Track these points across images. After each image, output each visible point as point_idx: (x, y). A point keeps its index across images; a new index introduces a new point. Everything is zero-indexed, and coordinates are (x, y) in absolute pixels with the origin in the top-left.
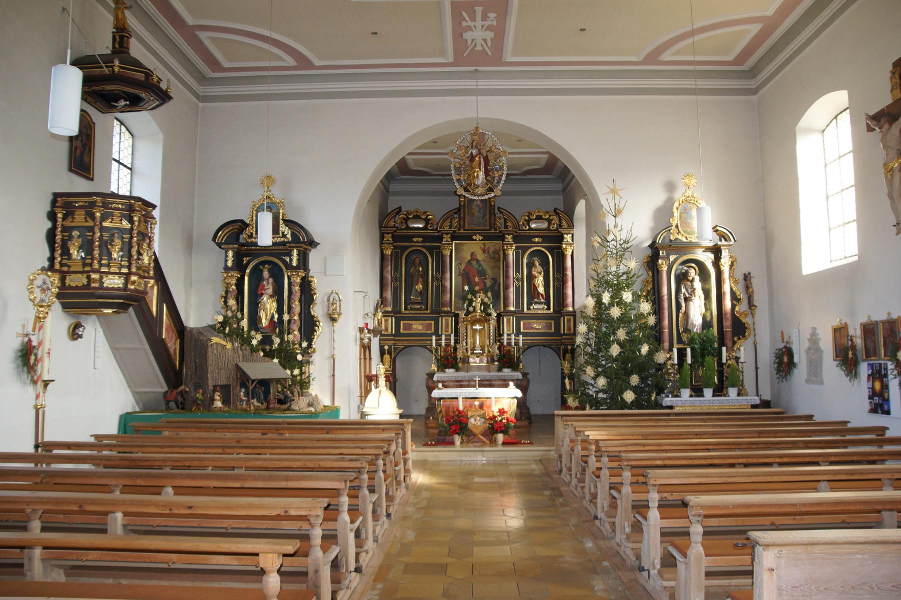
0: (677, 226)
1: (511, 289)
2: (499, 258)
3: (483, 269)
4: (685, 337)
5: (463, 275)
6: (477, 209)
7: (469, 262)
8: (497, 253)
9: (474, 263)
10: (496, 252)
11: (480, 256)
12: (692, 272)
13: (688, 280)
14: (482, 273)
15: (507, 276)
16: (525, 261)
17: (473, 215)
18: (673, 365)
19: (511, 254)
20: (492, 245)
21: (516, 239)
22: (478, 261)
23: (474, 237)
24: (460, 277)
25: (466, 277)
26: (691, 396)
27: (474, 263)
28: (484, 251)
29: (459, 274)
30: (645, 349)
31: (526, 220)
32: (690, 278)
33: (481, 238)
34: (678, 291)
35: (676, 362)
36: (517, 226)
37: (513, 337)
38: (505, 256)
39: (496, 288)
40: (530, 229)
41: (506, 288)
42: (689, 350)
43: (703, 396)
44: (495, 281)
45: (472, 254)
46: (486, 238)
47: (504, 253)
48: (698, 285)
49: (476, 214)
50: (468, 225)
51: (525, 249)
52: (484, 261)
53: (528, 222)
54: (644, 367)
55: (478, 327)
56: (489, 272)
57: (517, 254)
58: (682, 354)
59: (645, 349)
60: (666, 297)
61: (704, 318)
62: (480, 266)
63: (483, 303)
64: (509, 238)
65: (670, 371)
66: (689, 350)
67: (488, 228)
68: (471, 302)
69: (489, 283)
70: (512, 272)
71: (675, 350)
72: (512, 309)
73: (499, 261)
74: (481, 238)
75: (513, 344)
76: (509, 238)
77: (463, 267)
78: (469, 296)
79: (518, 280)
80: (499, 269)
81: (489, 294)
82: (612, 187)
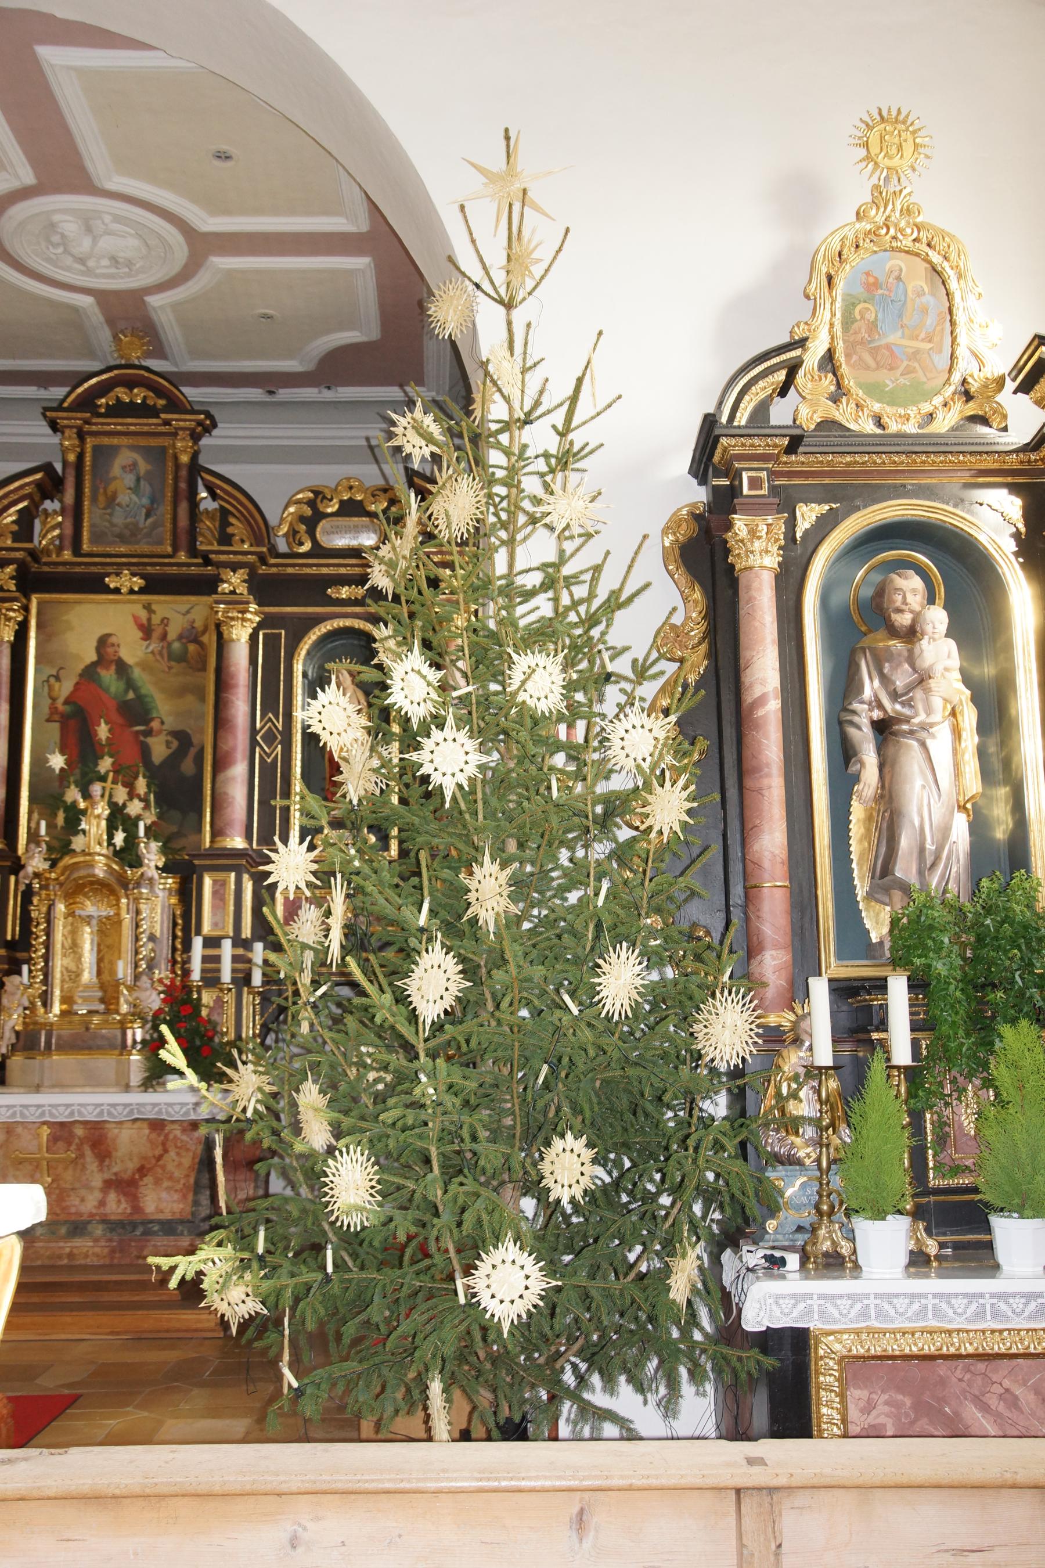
0: (829, 360)
1: (239, 770)
2: (201, 657)
3: (140, 698)
4: (877, 924)
5: (65, 721)
6: (129, 479)
7: (89, 673)
8: (196, 640)
9: (108, 676)
10: (191, 636)
11: (132, 649)
12: (910, 587)
13: (893, 632)
14: (135, 712)
15: (221, 722)
16: (298, 668)
17: (111, 500)
18: (814, 1072)
19: (240, 634)
20: (177, 612)
21: (265, 589)
22: (122, 668)
23: (112, 582)
24: (54, 730)
25: (74, 725)
26: (918, 1261)
27: (108, 676)
28: (146, 630)
29: (50, 715)
30: (622, 980)
31: (302, 519)
32: (904, 620)
33: (138, 582)
34: (843, 688)
35: (824, 1056)
36: (261, 530)
37: (227, 949)
38: (222, 644)
39: (188, 766)
40: (319, 551)
41: (221, 764)
42: (898, 989)
43: (993, 1268)
44: (183, 739)
45: (103, 642)
46: (155, 585)
47: (220, 635)
48: (940, 652)
49: (123, 498)
50: (97, 537)
51: (300, 628)
52: (144, 665)
53: (312, 521)
54: (634, 1096)
55: (91, 908)
56: (166, 711)
57: (272, 643)
58: (859, 1013)
59: (622, 980)
60: (771, 710)
61: (979, 826)
62: (130, 684)
63: (117, 817)
64: (235, 581)
65: (796, 1109)
66: (898, 989)
67: (169, 549)
68: (74, 816)
69: (159, 749)
70: (240, 708)
71: (819, 989)
72: (238, 843)
73: (204, 668)
74: (138, 582)
75: (226, 976)
76: (235, 581)
77: (65, 688)
78: (73, 794)
79: (269, 738)
80: (203, 699)
81: (141, 785)
82: (497, 162)
